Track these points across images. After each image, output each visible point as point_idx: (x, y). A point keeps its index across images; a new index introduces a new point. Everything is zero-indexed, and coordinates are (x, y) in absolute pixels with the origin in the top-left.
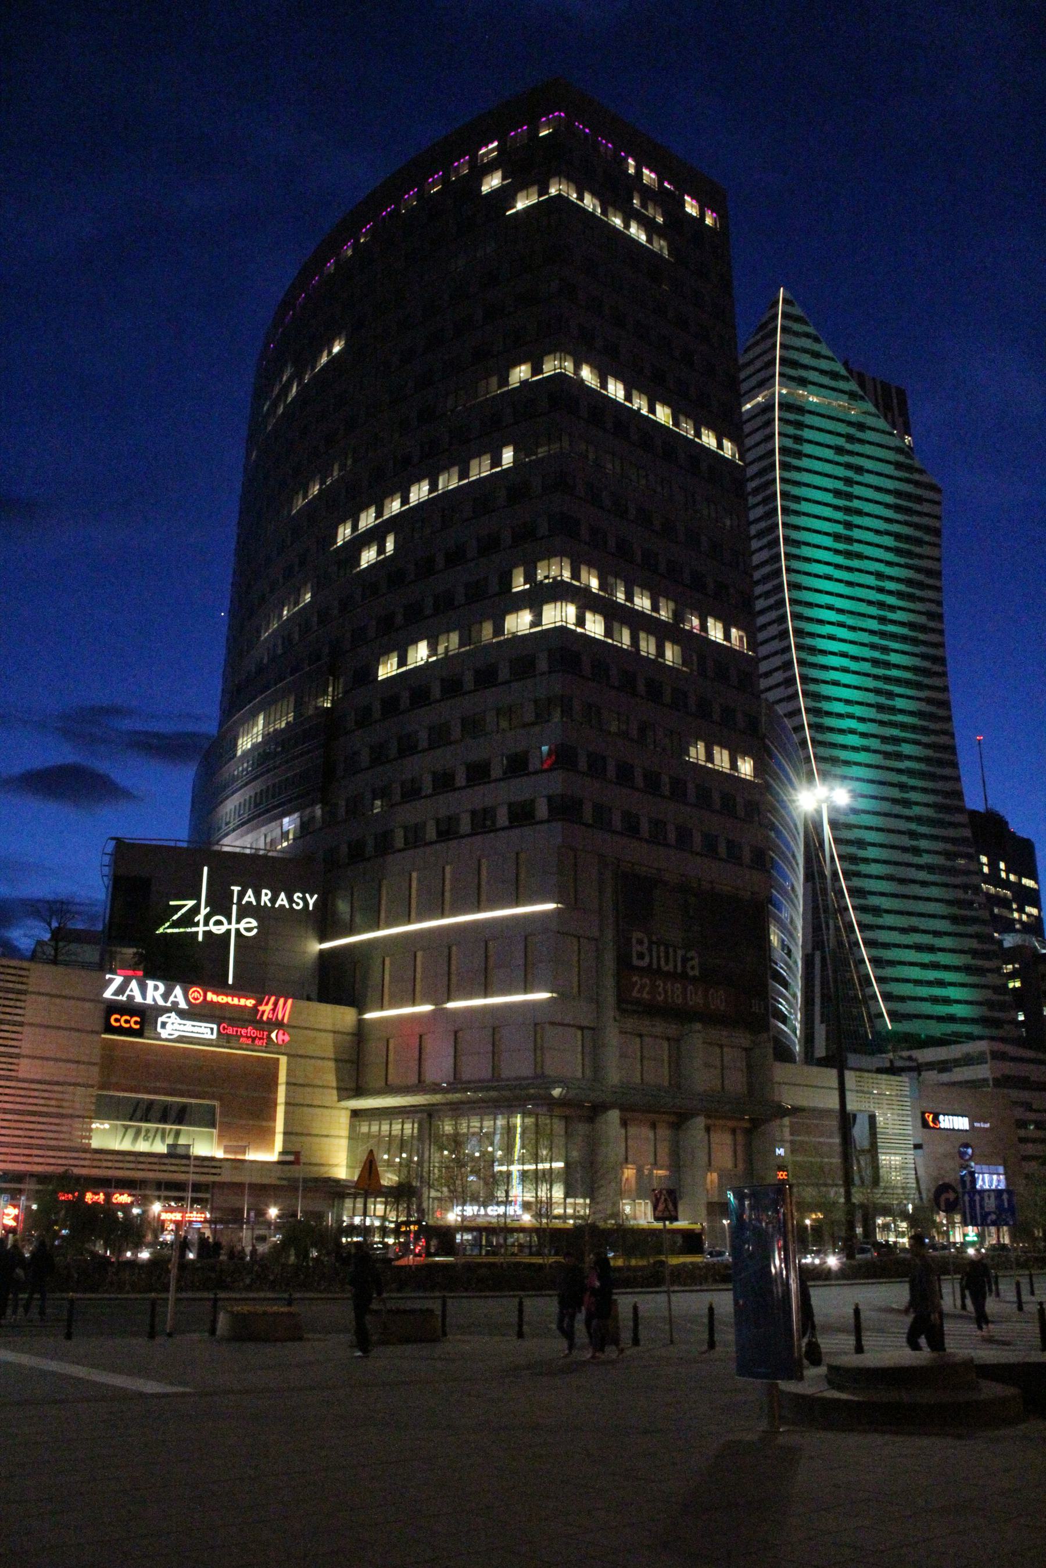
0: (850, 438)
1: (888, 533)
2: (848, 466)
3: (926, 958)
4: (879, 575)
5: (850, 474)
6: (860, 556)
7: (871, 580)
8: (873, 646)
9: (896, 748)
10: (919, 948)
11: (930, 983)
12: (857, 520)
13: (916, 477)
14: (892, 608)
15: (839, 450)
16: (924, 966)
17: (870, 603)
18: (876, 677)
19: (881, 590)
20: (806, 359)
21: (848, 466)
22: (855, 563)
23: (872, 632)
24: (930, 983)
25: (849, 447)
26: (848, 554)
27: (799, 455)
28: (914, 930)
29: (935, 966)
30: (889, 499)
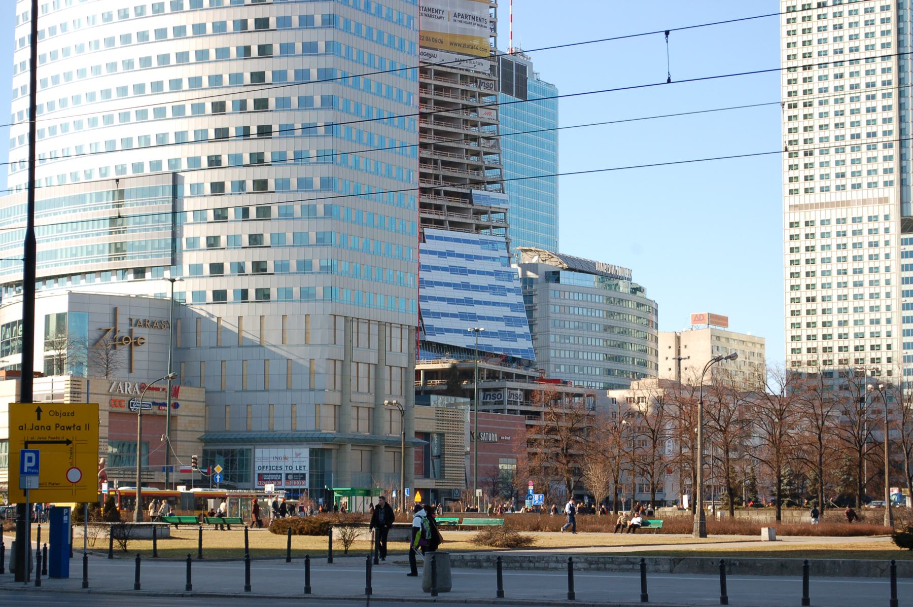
3: (458, 279)
10: (453, 270)
11: (459, 302)
16: (456, 286)
24: (459, 302)
28: (451, 254)
29: (466, 286)
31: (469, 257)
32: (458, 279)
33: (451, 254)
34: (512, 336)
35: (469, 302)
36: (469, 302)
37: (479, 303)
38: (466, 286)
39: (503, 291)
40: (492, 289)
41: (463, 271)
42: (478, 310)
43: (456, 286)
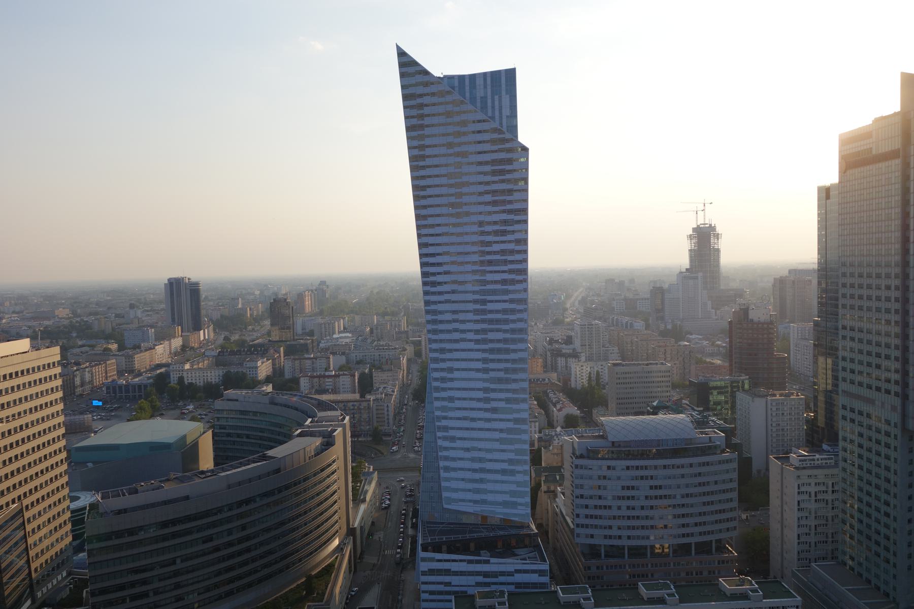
0: (458, 134)
1: (487, 192)
2: (458, 154)
4: (481, 224)
5: (459, 159)
6: (468, 214)
7: (475, 228)
8: (474, 272)
9: (483, 336)
10: (473, 460)
12: (465, 190)
13: (508, 145)
14: (489, 244)
15: (450, 145)
16: (475, 471)
17: (474, 243)
18: (474, 292)
19: (483, 233)
20: (420, 90)
21: (458, 154)
22: (465, 219)
23: (475, 263)
25: (457, 140)
26: (458, 215)
27: (423, 157)
29: (482, 470)
30: (488, 168)
31: (489, 451)
32: (477, 465)
33: (474, 449)
34: (514, 505)
35: (481, 481)
36: (481, 481)
37: (489, 481)
38: (482, 470)
39: (513, 473)
40: (504, 472)
41: (481, 460)
42: (489, 486)
43: (475, 471)
